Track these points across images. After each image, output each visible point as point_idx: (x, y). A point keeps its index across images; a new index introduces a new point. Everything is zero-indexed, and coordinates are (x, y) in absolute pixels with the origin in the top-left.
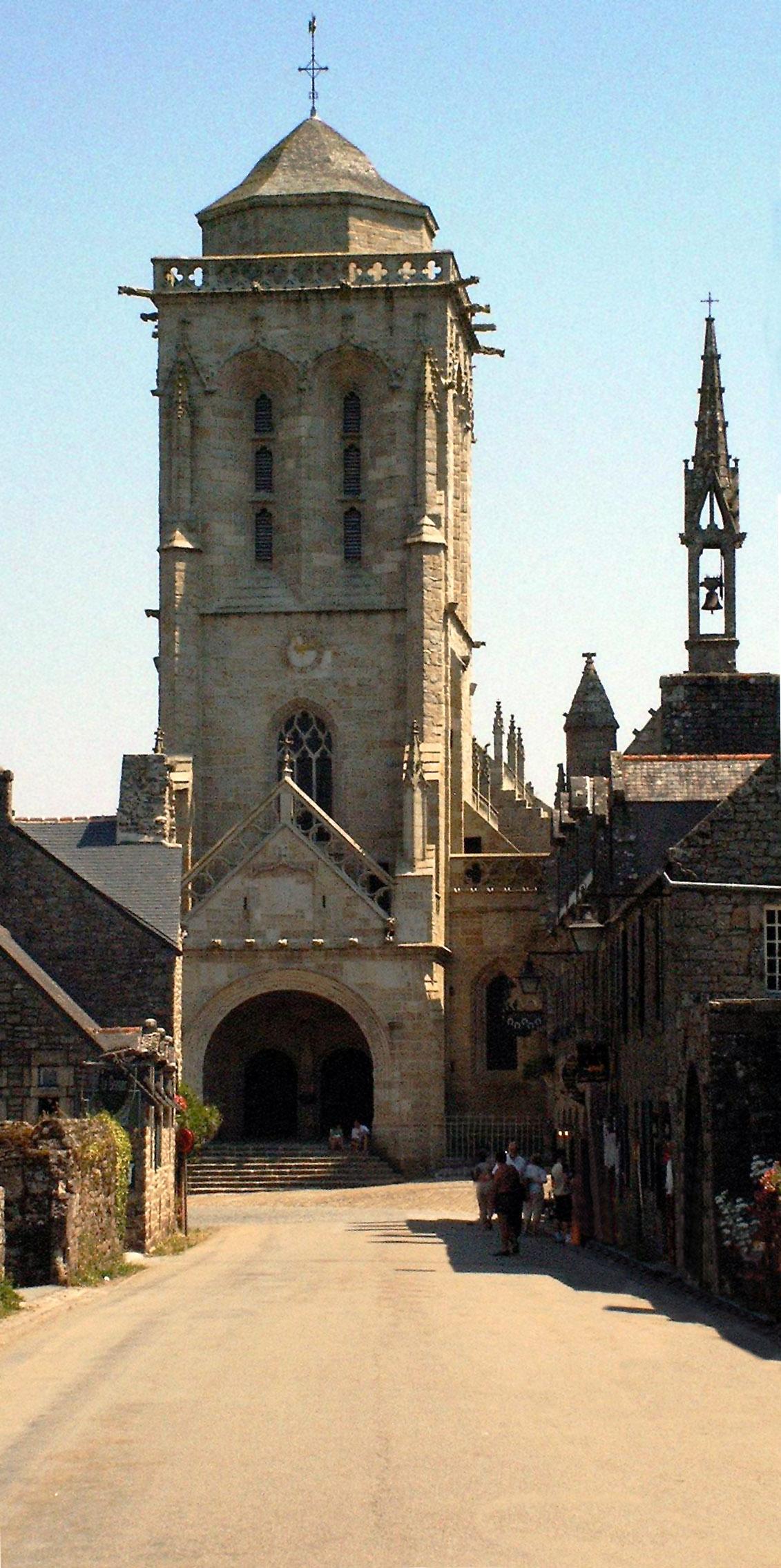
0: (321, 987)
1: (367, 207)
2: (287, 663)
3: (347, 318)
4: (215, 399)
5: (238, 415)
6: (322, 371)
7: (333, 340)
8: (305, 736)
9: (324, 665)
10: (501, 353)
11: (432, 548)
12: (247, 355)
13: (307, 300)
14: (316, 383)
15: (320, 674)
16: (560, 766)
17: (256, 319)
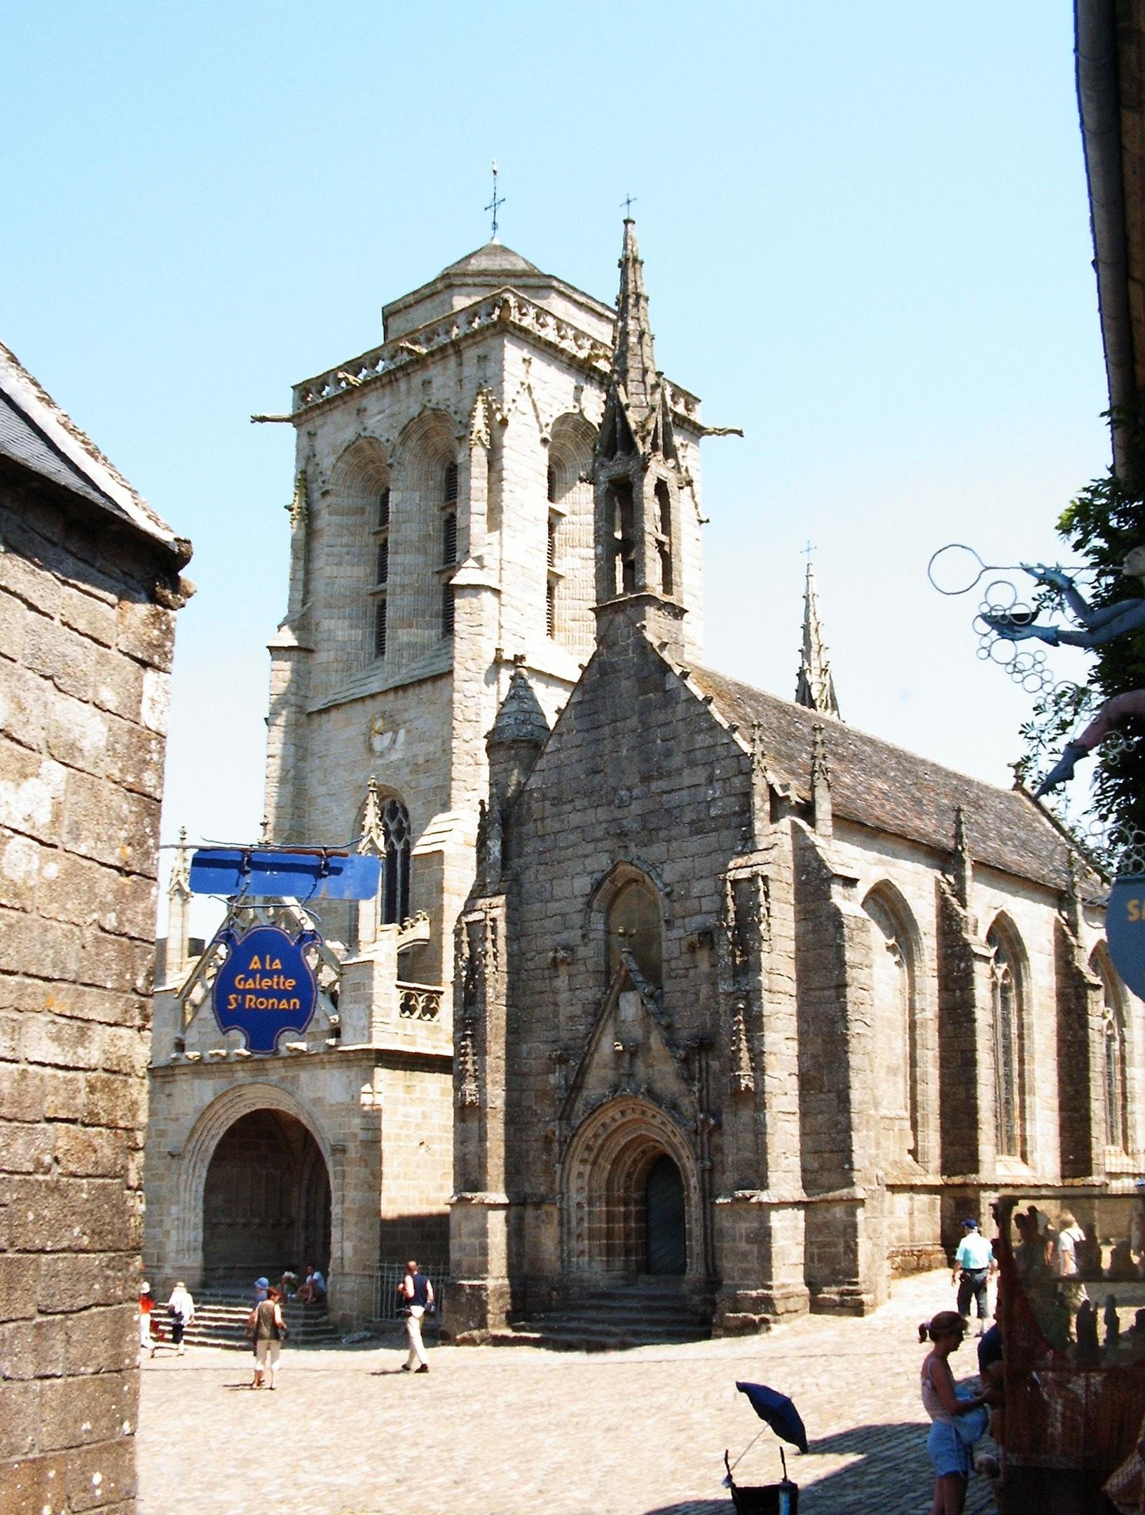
0: (286, 1105)
1: (475, 285)
2: (370, 749)
3: (427, 383)
4: (329, 499)
5: (362, 511)
6: (411, 444)
7: (415, 410)
8: (392, 827)
9: (398, 746)
10: (740, 433)
11: (469, 591)
12: (353, 448)
13: (397, 380)
14: (408, 457)
15: (395, 756)
16: (482, 803)
17: (360, 411)
